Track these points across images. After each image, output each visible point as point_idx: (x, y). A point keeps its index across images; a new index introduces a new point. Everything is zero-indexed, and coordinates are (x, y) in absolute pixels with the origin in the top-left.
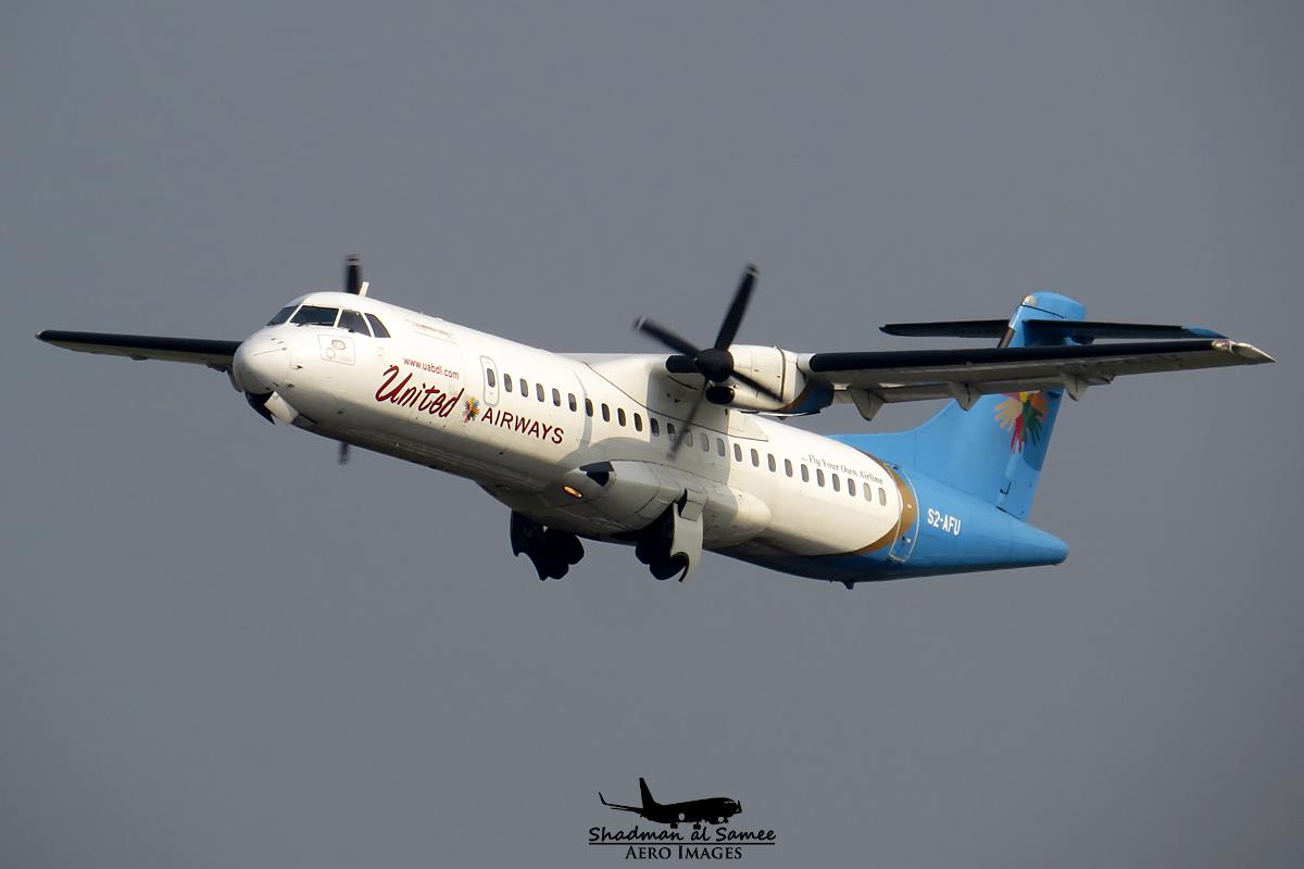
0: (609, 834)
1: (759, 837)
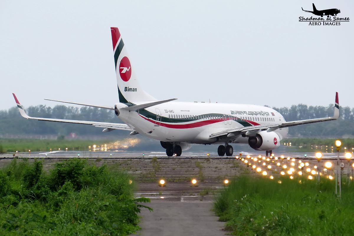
0: (304, 18)
1: (345, 19)
